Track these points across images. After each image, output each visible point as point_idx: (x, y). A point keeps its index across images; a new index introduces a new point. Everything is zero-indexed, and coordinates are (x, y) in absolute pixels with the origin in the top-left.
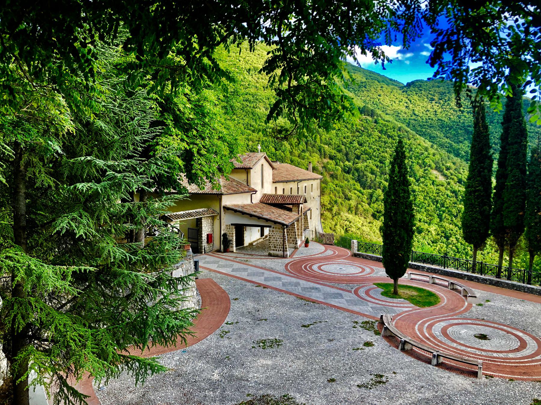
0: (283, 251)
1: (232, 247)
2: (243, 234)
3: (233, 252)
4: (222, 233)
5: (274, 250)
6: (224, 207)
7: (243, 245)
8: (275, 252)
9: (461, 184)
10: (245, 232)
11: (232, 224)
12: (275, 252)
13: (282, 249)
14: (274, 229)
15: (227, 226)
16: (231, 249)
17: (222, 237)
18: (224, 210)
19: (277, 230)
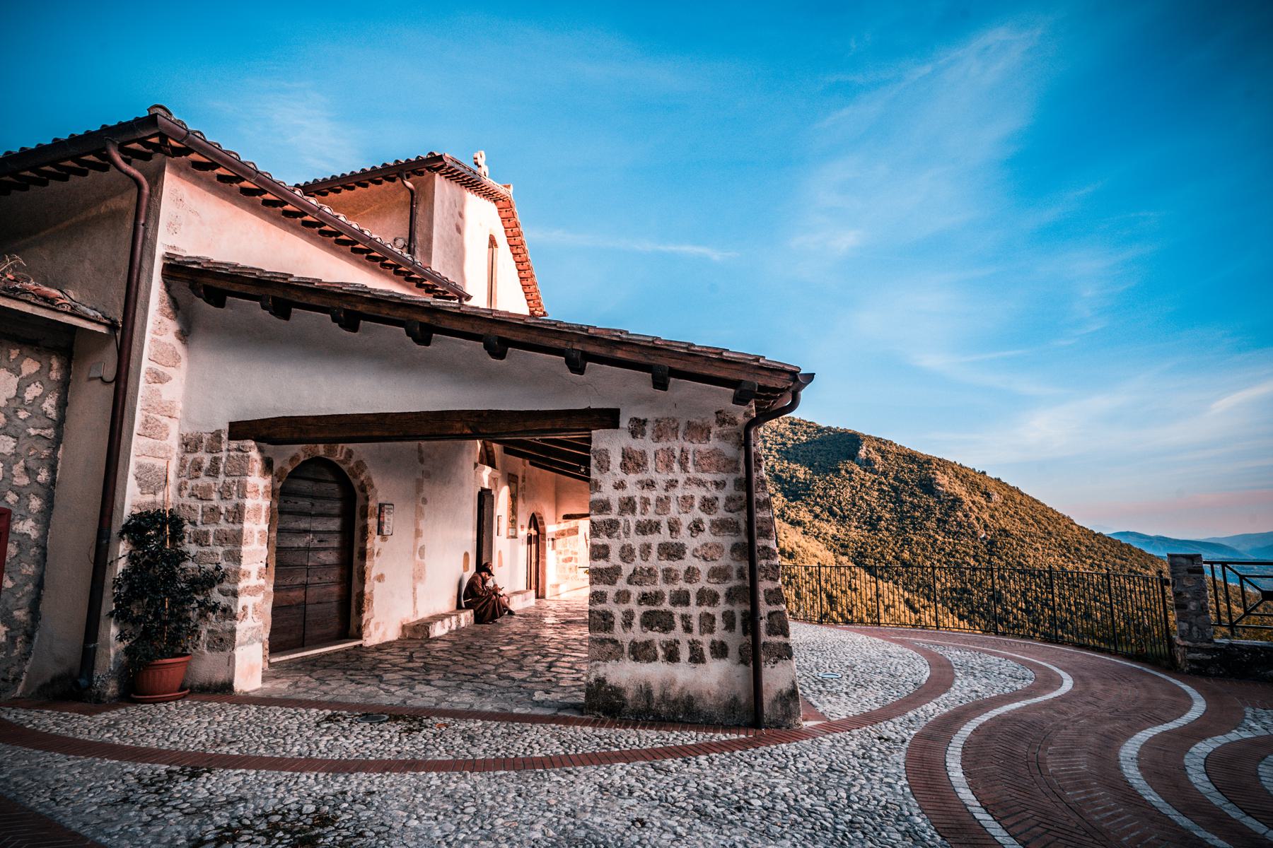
0: (753, 657)
1: (225, 642)
2: (363, 555)
3: (224, 690)
4: (133, 498)
5: (641, 652)
6: (176, 270)
7: (360, 638)
8: (655, 672)
9: (785, 556)
10: (374, 542)
11: (239, 430)
12: (655, 672)
13: (734, 640)
14: (646, 444)
15: (189, 444)
16: (206, 666)
17: (123, 548)
18: (177, 307)
19: (676, 445)
